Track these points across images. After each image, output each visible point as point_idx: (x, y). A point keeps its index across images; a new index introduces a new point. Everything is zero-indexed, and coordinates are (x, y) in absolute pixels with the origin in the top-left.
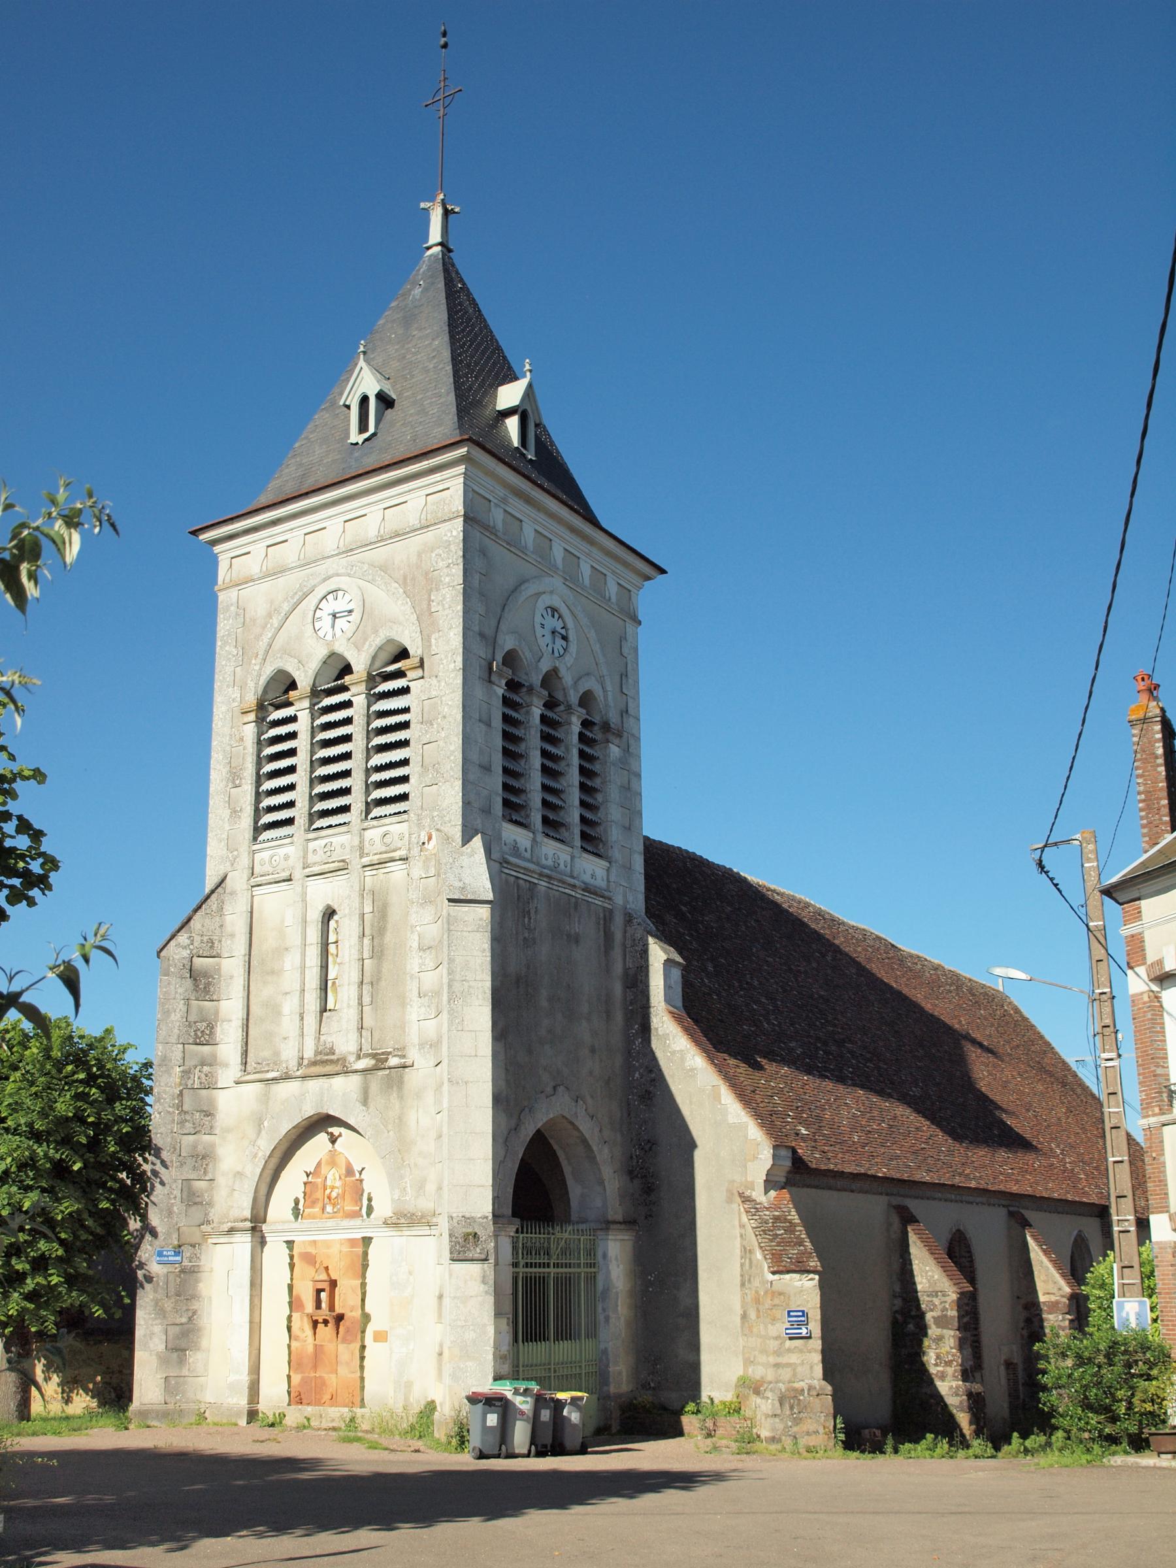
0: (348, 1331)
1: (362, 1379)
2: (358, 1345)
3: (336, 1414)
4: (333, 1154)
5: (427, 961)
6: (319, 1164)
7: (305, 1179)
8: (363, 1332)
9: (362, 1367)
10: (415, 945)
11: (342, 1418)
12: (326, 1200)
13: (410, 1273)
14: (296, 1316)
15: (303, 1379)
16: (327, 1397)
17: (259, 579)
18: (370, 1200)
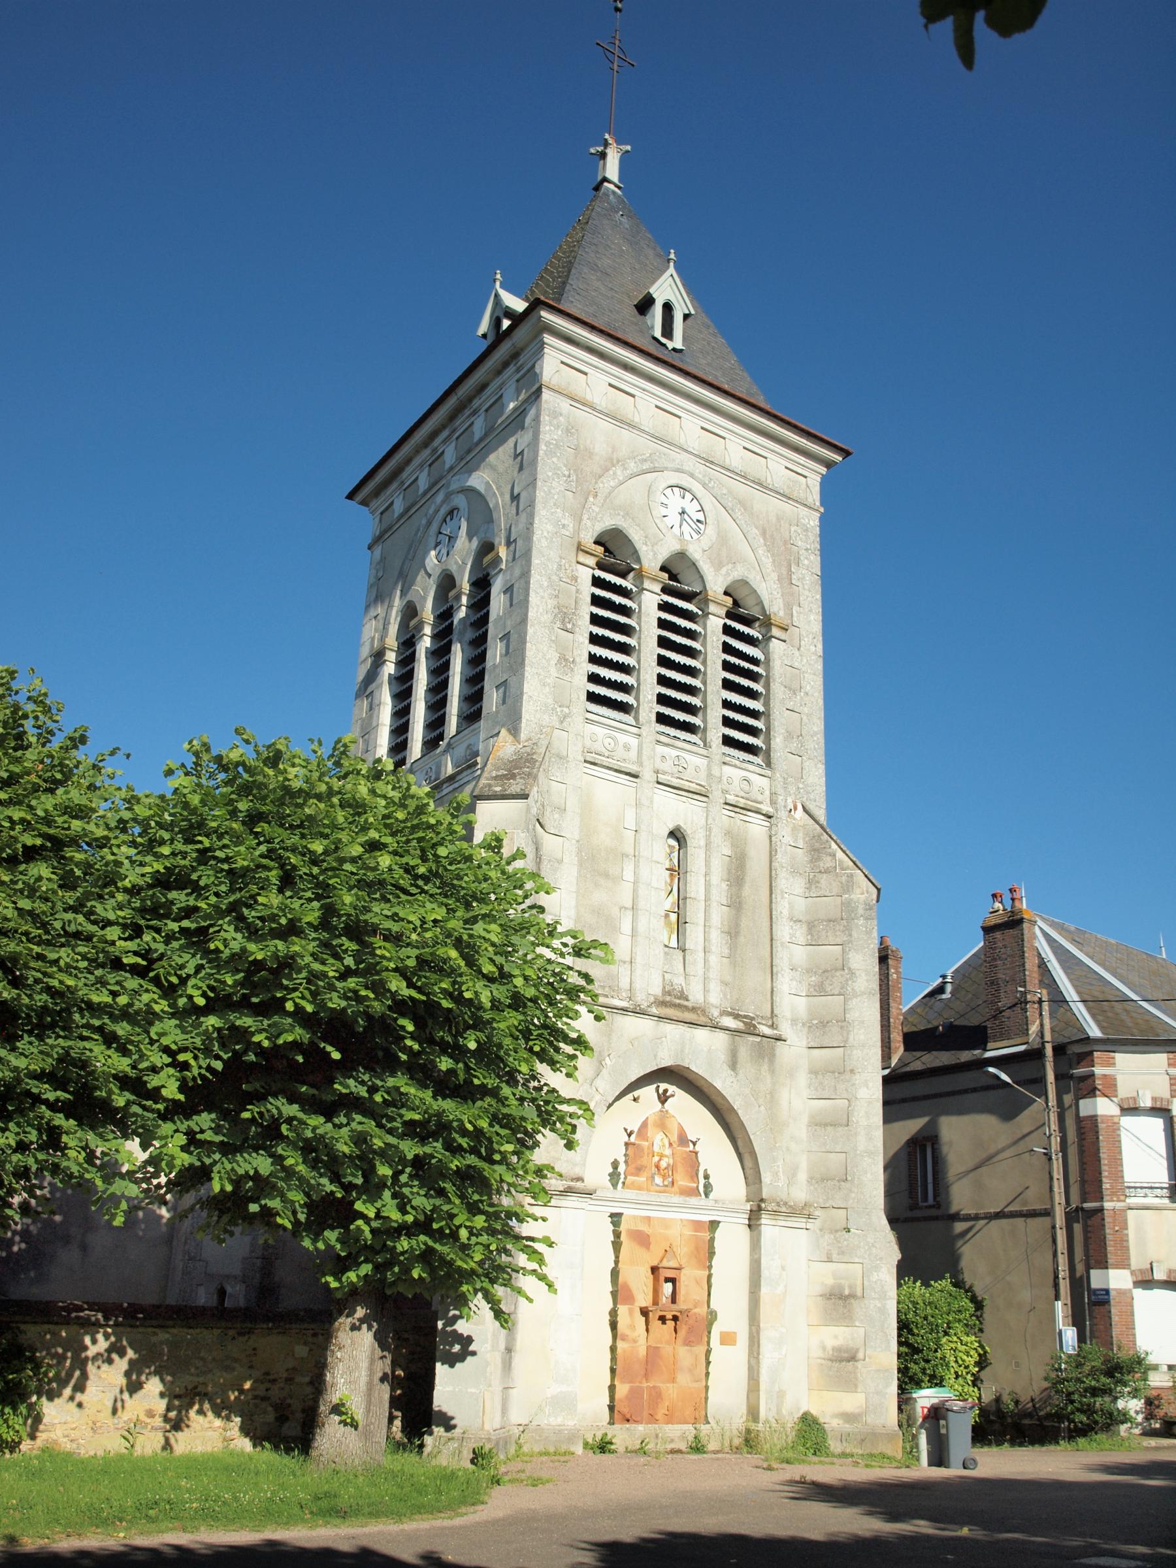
0: (690, 1330)
1: (707, 1388)
2: (704, 1348)
3: (678, 1433)
4: (663, 1115)
5: (798, 934)
6: (645, 1125)
7: (626, 1138)
8: (709, 1333)
9: (707, 1374)
10: (786, 912)
11: (683, 1437)
12: (654, 1169)
13: (783, 1268)
14: (622, 1310)
16: (660, 1413)
18: (706, 1177)
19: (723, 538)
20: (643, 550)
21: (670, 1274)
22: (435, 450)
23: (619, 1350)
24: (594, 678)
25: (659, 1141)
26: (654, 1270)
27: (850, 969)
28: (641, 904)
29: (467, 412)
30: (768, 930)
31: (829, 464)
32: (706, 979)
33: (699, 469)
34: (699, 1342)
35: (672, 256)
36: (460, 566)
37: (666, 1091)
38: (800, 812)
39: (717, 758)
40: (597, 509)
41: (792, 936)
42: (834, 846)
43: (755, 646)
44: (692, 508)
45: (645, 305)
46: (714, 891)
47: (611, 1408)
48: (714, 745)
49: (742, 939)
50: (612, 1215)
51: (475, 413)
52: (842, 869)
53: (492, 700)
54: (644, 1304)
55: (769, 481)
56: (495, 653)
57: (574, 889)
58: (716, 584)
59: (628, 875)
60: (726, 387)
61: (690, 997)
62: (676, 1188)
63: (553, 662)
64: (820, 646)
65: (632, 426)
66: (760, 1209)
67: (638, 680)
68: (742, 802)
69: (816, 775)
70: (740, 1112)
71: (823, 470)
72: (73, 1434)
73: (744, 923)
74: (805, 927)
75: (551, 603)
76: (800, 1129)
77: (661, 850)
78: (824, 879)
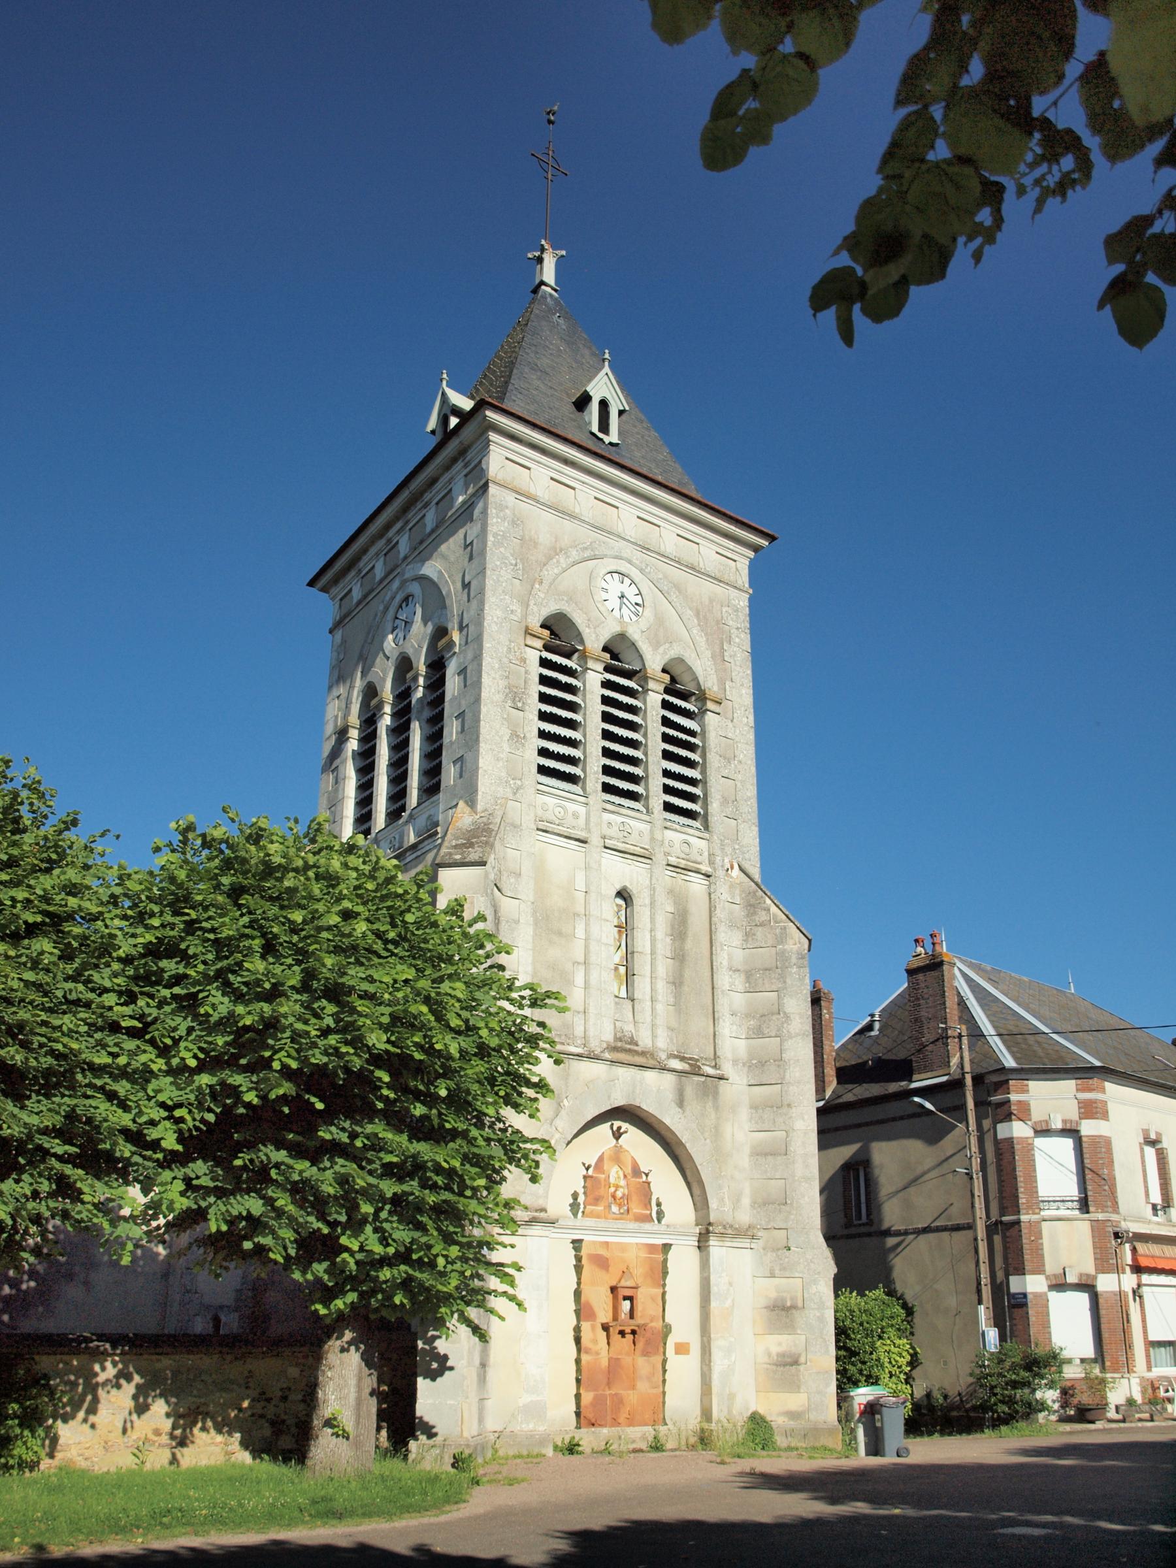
0: (648, 1343)
1: (664, 1393)
3: (639, 1434)
6: (601, 1159)
7: (584, 1172)
8: (665, 1344)
9: (664, 1381)
10: (725, 963)
11: (644, 1437)
12: (611, 1199)
13: (730, 1284)
14: (585, 1326)
15: (596, 1398)
17: (543, 504)
18: (659, 1204)
19: (660, 620)
20: (586, 632)
21: (628, 1293)
22: (389, 541)
23: (583, 1362)
24: (543, 752)
25: (614, 1174)
26: (613, 1289)
27: (785, 1013)
28: (593, 958)
29: (419, 505)
30: (709, 978)
31: (756, 549)
32: (653, 1026)
33: (637, 555)
34: (656, 1353)
35: (607, 356)
36: (416, 650)
37: (619, 1128)
38: (736, 872)
39: (659, 823)
40: (542, 596)
41: (732, 984)
42: (768, 901)
43: (692, 719)
44: (631, 592)
45: (583, 402)
46: (659, 945)
47: (578, 1414)
48: (656, 812)
49: (686, 988)
50: (574, 1242)
51: (426, 505)
52: (776, 922)
53: (449, 774)
54: (605, 1321)
55: (701, 565)
56: (452, 730)
57: (530, 946)
58: (654, 662)
59: (580, 932)
60: (660, 478)
61: (640, 1043)
62: (631, 1216)
63: (506, 738)
64: (751, 718)
65: (572, 516)
66: (708, 1232)
67: (584, 753)
68: (683, 863)
69: (750, 837)
70: (688, 1145)
71: (751, 554)
72: (87, 1453)
73: (688, 974)
74: (743, 976)
75: (502, 683)
76: (744, 1159)
77: (610, 909)
78: (759, 931)
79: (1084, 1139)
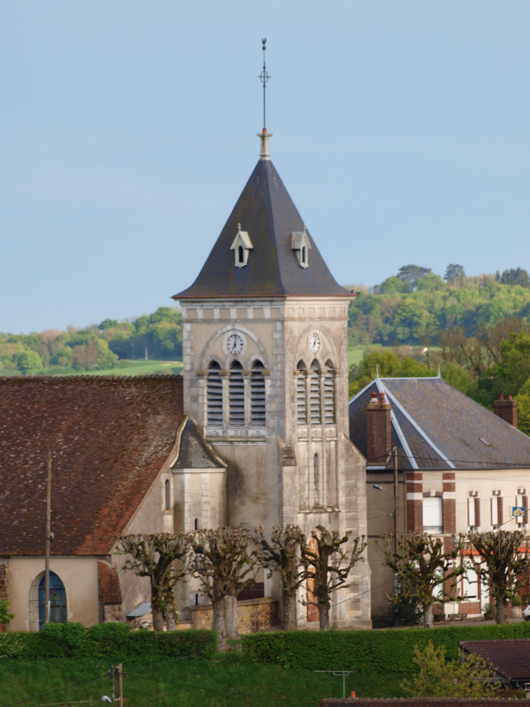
32: (323, 499)
78: (350, 459)
79: (444, 501)
